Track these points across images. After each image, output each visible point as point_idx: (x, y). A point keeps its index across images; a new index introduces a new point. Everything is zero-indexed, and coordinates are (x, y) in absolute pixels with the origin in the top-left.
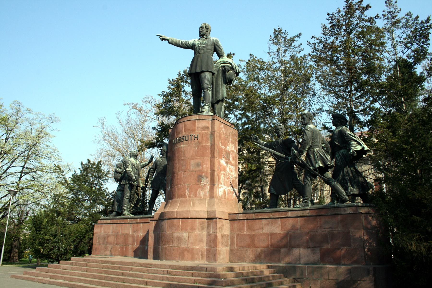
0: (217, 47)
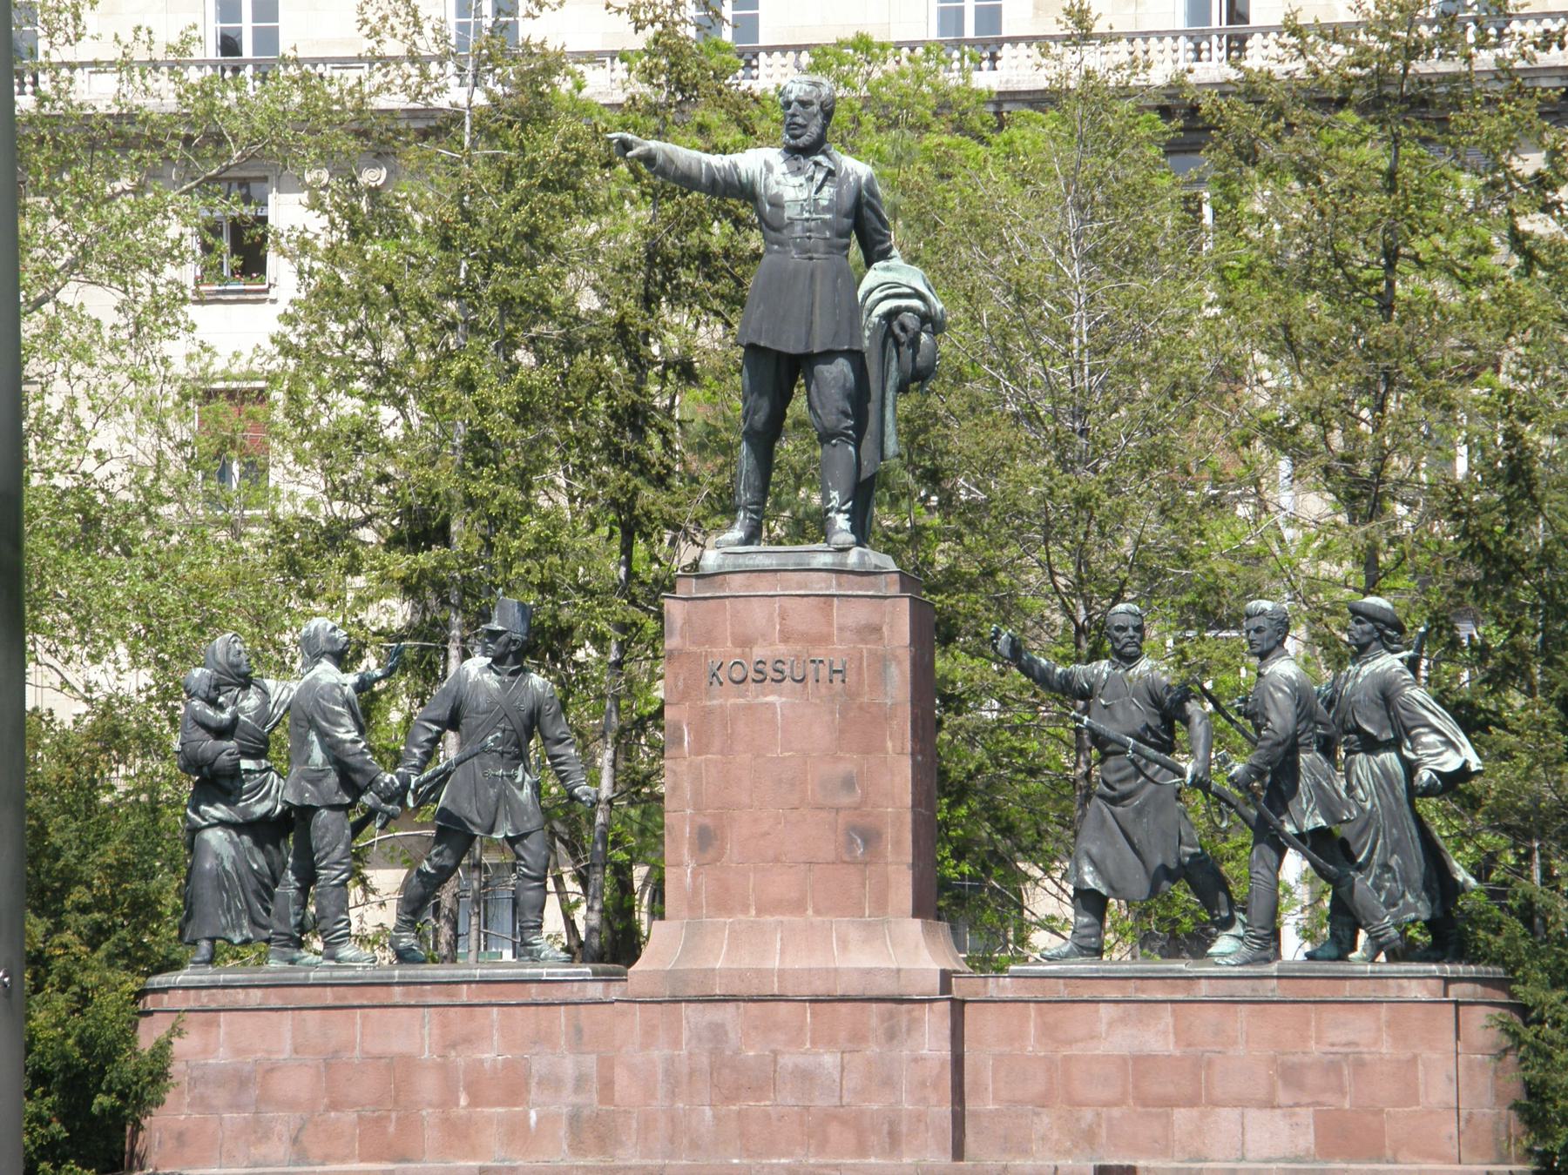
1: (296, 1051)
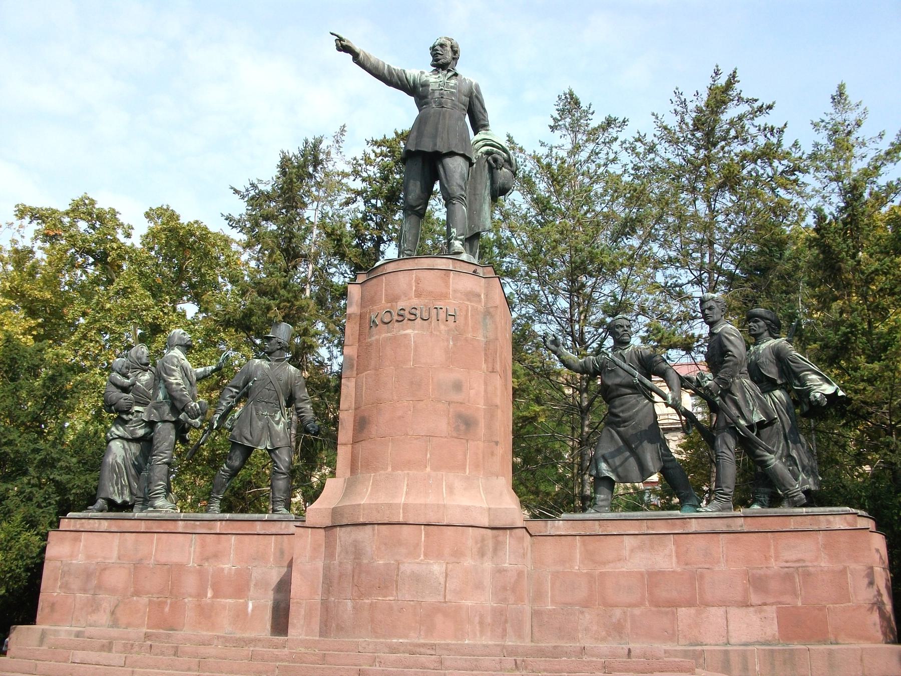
1: (119, 558)
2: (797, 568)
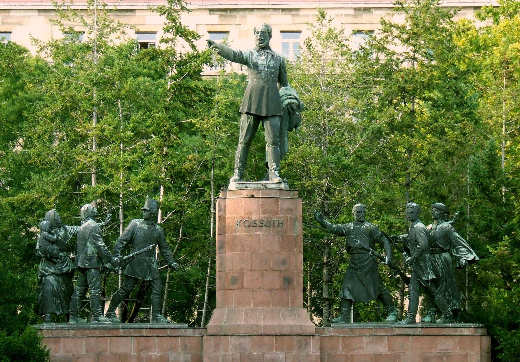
0: (283, 70)
1: (87, 352)
2: (445, 353)
